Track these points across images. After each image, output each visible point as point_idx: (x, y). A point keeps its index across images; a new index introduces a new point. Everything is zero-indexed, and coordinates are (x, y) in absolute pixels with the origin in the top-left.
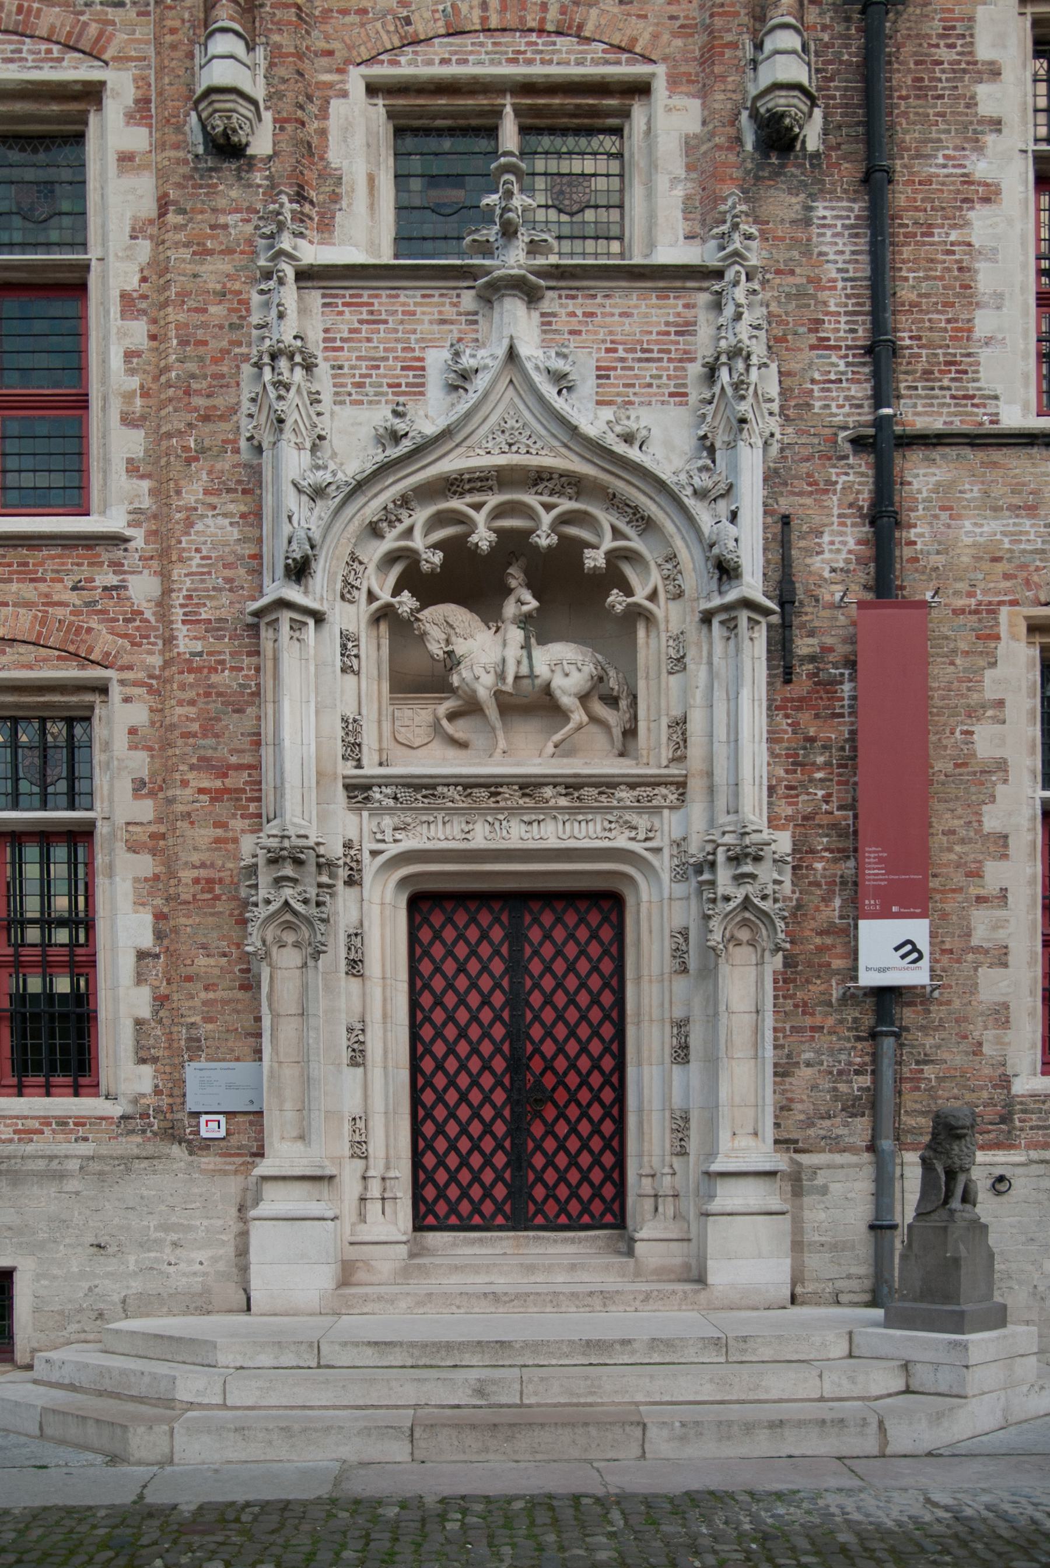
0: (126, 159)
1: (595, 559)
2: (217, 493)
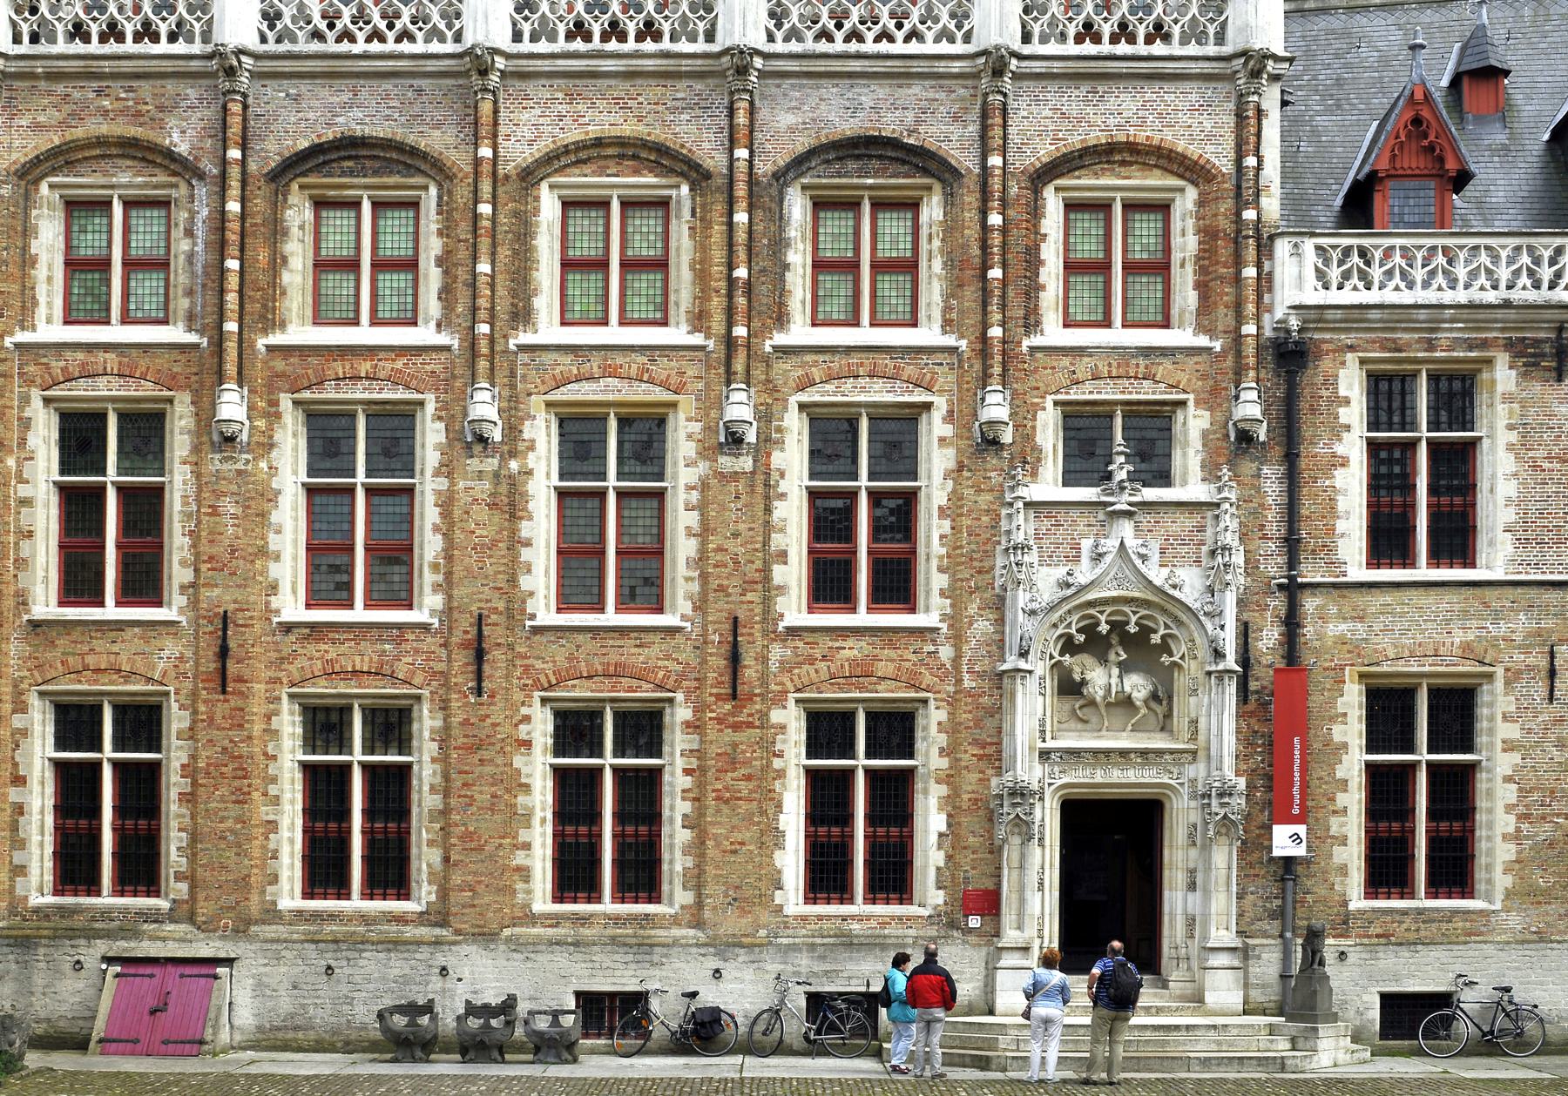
0: (942, 440)
1: (1156, 639)
2: (984, 609)
